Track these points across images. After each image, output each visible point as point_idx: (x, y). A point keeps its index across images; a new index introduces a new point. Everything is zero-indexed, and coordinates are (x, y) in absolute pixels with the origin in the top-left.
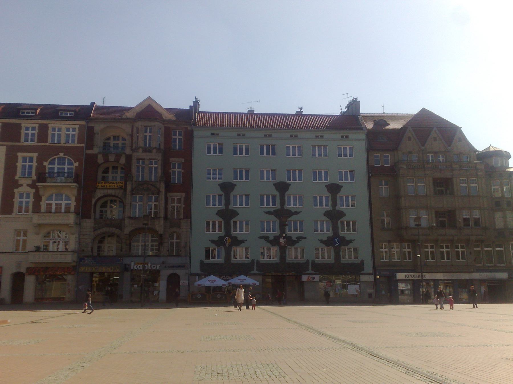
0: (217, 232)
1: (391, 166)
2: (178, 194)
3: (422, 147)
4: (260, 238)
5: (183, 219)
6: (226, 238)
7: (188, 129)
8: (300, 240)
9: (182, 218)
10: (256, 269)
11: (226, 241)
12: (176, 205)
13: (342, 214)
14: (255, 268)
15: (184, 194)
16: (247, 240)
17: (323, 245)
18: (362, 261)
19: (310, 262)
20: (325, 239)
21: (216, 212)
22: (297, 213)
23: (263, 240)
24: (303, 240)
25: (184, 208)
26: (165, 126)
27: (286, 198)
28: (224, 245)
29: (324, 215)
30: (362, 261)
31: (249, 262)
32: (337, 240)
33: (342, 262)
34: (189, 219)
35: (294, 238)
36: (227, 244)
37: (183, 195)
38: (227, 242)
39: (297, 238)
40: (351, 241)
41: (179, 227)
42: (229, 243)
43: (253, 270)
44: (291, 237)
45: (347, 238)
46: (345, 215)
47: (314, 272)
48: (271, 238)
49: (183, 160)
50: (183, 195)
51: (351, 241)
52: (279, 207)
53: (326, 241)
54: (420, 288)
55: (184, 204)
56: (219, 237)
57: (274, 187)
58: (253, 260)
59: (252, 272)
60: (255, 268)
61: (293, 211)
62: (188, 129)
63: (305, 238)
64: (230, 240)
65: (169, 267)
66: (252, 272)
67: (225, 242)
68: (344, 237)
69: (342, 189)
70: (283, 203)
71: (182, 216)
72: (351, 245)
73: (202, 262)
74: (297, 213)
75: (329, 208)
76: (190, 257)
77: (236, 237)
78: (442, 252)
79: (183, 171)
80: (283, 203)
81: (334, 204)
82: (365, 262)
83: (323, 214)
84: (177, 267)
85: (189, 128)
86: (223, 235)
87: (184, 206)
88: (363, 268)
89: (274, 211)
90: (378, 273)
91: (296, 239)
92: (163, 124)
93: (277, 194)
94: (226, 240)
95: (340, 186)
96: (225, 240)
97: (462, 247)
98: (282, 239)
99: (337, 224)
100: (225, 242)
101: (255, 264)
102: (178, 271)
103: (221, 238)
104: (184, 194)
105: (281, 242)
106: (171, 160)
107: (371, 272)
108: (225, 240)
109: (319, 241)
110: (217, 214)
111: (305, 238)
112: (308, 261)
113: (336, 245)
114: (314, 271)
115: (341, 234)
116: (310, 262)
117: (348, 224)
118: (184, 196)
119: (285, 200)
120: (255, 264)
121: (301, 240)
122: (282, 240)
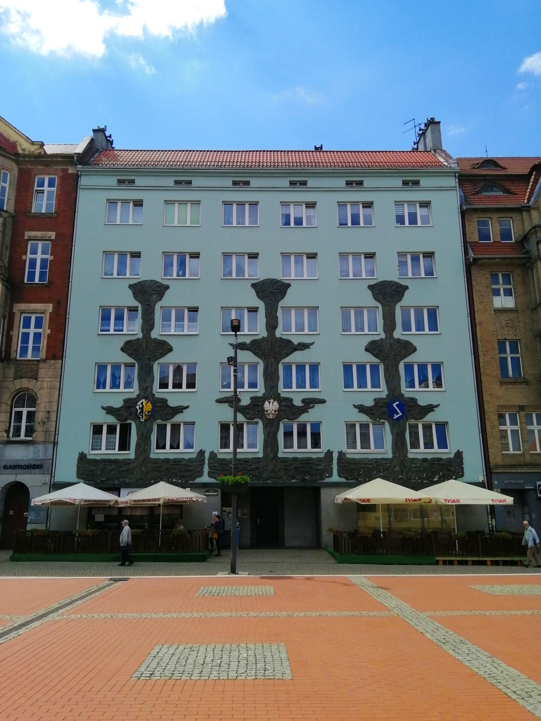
0: (122, 389)
1: (516, 242)
2: (39, 306)
4: (219, 401)
5: (46, 359)
6: (141, 402)
7: (70, 172)
8: (311, 405)
9: (44, 357)
10: (209, 472)
11: (142, 409)
12: (32, 330)
14: (206, 469)
15: (51, 305)
16: (188, 407)
17: (365, 418)
18: (459, 455)
19: (335, 456)
20: (369, 403)
21: (121, 345)
22: (304, 346)
23: (226, 405)
24: (317, 406)
25: (49, 336)
26: (21, 167)
27: (280, 314)
28: (136, 418)
29: (367, 350)
30: (459, 455)
31: (194, 456)
32: (396, 405)
33: (410, 456)
34: (60, 361)
35: (298, 402)
36: (143, 417)
37: (49, 307)
38: (142, 412)
39: (303, 401)
41: (35, 377)
42: (146, 413)
43: (201, 474)
44: (290, 400)
46: (415, 350)
47: (343, 480)
48: (245, 401)
49: (52, 235)
50: (49, 307)
52: (264, 334)
53: (371, 407)
55: (49, 329)
56: (126, 401)
57: (253, 292)
58: (201, 453)
59: (199, 480)
60: (206, 469)
61: (296, 341)
62: (70, 172)
63: (323, 401)
64: (148, 407)
65: (5, 467)
66: (199, 480)
67: (139, 411)
68: (414, 400)
69: (407, 293)
70: (272, 324)
71: (43, 354)
72: (430, 418)
73: (82, 457)
74: (304, 346)
75: (380, 334)
76: (55, 444)
77: (165, 401)
79: (52, 258)
80: (272, 324)
81: (390, 326)
82: (464, 455)
84: (24, 469)
85: (71, 170)
86: (134, 396)
87: (49, 332)
88: (462, 469)
89: (254, 342)
90: (496, 482)
91: (301, 405)
92: (18, 163)
93: (261, 305)
94: (141, 406)
95: (402, 286)
96: (138, 407)
98: (269, 403)
99: (397, 370)
100: (139, 411)
101: (206, 462)
102: (26, 478)
103: (130, 404)
104: (51, 305)
105: (267, 411)
106: (28, 234)
107: (481, 481)
108: (138, 407)
110: (123, 349)
111: (323, 401)
112: (329, 454)
113: (396, 417)
115: (406, 391)
116: (335, 456)
117: (423, 368)
118: (50, 310)
119: (276, 318)
120: (206, 462)
121: (313, 407)
122: (271, 407)
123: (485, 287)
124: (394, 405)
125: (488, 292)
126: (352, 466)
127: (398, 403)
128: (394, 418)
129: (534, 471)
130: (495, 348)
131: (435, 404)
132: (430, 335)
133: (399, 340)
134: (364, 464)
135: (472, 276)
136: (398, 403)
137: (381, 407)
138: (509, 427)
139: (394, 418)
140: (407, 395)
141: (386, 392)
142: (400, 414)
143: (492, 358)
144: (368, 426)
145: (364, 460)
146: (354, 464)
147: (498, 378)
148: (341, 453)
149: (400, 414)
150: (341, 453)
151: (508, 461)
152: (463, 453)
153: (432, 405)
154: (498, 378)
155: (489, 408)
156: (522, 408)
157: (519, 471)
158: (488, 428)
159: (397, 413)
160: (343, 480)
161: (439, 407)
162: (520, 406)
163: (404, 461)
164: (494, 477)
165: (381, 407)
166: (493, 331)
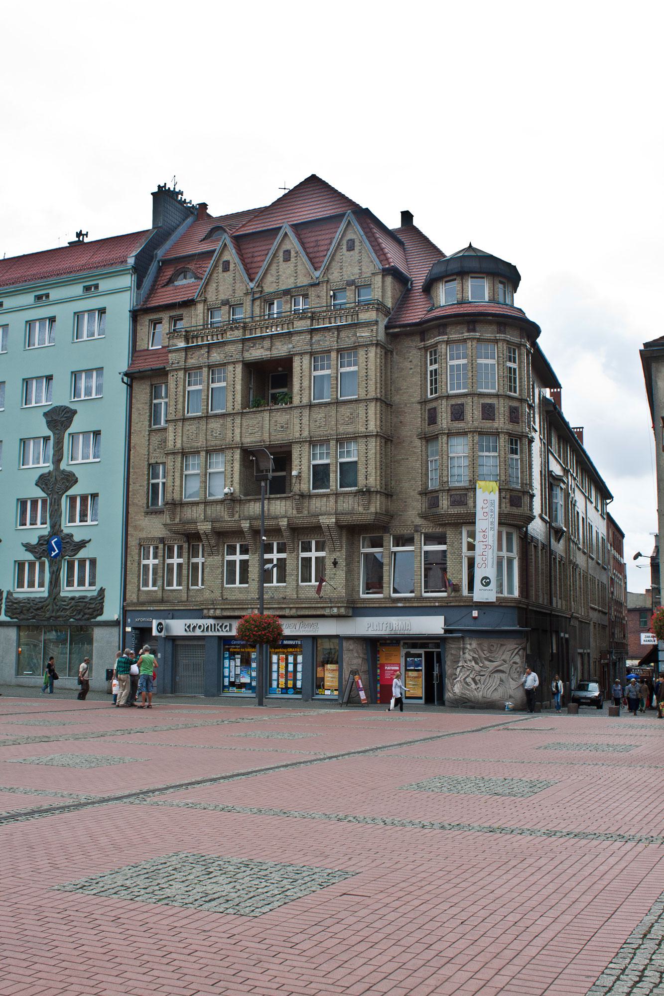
3: (250, 284)
13: (70, 479)
17: (30, 557)
18: (102, 591)
30: (102, 591)
40: (83, 544)
45: (77, 538)
47: (8, 619)
51: (83, 544)
54: (224, 658)
69: (76, 418)
72: (82, 554)
75: (47, 466)
78: (307, 561)
82: (106, 593)
83: (35, 483)
88: (102, 608)
90: (129, 620)
97: (244, 551)
109: (24, 546)
113: (53, 554)
114: (9, 616)
115: (67, 527)
123: (143, 403)
124: (53, 542)
125: (146, 410)
126: (15, 605)
127: (56, 539)
128: (52, 555)
129: (162, 608)
130: (145, 474)
131: (87, 539)
132: (90, 464)
133: (64, 471)
134: (24, 603)
135: (133, 392)
136: (56, 539)
137: (42, 544)
138: (151, 562)
139: (52, 555)
140: (66, 531)
141: (49, 529)
142: (57, 551)
143: (140, 486)
144: (34, 564)
145: (29, 599)
146: (16, 603)
147: (143, 507)
148: (9, 593)
149: (57, 551)
150: (9, 593)
151: (143, 598)
152: (106, 591)
153: (84, 540)
154: (143, 507)
155: (133, 542)
156: (162, 540)
157: (149, 608)
158: (129, 563)
159: (55, 551)
160: (8, 619)
161: (90, 543)
162: (160, 538)
163: (56, 600)
164: (128, 614)
165: (42, 544)
166: (145, 455)
